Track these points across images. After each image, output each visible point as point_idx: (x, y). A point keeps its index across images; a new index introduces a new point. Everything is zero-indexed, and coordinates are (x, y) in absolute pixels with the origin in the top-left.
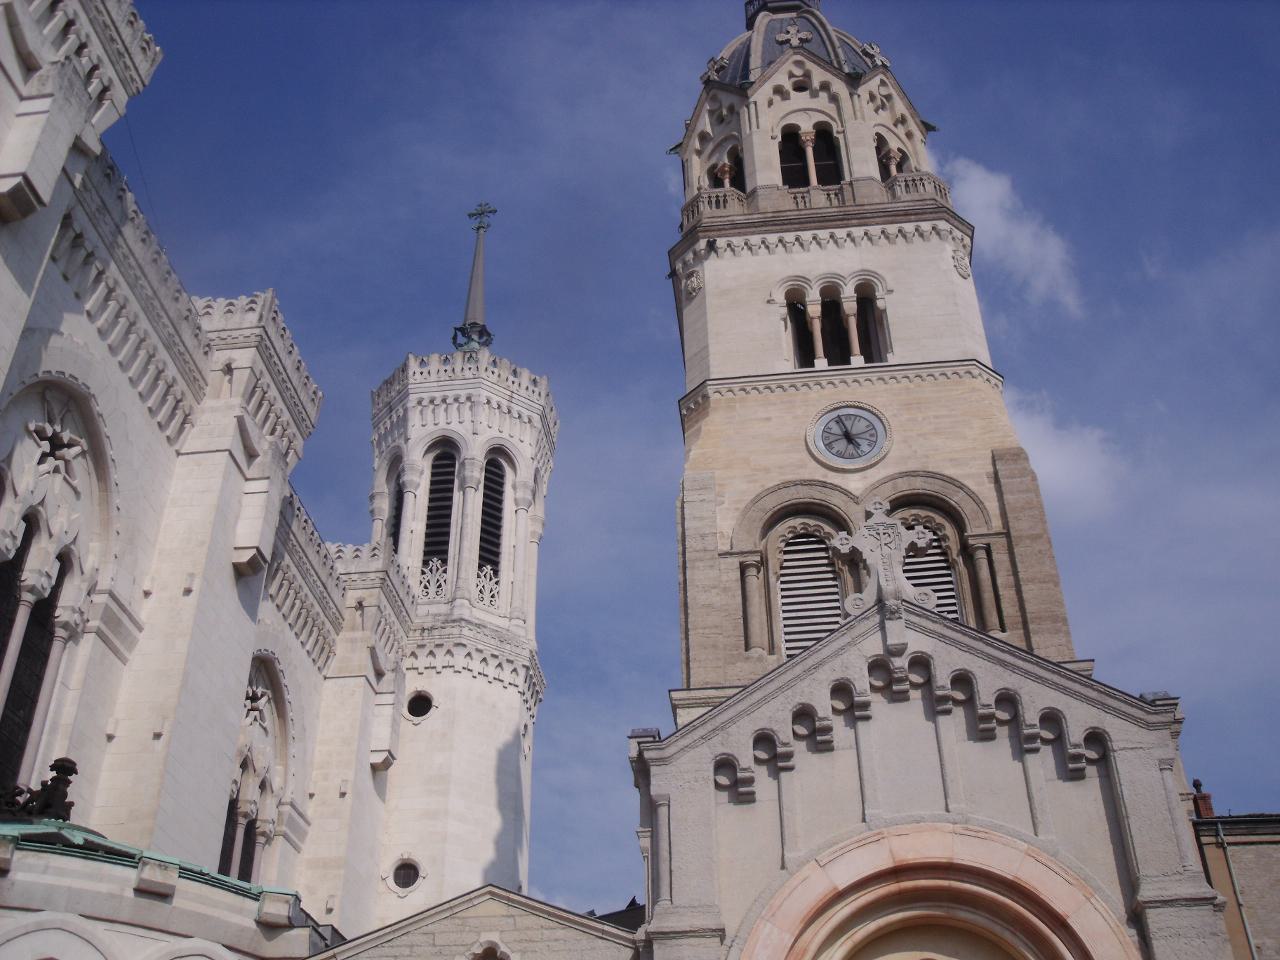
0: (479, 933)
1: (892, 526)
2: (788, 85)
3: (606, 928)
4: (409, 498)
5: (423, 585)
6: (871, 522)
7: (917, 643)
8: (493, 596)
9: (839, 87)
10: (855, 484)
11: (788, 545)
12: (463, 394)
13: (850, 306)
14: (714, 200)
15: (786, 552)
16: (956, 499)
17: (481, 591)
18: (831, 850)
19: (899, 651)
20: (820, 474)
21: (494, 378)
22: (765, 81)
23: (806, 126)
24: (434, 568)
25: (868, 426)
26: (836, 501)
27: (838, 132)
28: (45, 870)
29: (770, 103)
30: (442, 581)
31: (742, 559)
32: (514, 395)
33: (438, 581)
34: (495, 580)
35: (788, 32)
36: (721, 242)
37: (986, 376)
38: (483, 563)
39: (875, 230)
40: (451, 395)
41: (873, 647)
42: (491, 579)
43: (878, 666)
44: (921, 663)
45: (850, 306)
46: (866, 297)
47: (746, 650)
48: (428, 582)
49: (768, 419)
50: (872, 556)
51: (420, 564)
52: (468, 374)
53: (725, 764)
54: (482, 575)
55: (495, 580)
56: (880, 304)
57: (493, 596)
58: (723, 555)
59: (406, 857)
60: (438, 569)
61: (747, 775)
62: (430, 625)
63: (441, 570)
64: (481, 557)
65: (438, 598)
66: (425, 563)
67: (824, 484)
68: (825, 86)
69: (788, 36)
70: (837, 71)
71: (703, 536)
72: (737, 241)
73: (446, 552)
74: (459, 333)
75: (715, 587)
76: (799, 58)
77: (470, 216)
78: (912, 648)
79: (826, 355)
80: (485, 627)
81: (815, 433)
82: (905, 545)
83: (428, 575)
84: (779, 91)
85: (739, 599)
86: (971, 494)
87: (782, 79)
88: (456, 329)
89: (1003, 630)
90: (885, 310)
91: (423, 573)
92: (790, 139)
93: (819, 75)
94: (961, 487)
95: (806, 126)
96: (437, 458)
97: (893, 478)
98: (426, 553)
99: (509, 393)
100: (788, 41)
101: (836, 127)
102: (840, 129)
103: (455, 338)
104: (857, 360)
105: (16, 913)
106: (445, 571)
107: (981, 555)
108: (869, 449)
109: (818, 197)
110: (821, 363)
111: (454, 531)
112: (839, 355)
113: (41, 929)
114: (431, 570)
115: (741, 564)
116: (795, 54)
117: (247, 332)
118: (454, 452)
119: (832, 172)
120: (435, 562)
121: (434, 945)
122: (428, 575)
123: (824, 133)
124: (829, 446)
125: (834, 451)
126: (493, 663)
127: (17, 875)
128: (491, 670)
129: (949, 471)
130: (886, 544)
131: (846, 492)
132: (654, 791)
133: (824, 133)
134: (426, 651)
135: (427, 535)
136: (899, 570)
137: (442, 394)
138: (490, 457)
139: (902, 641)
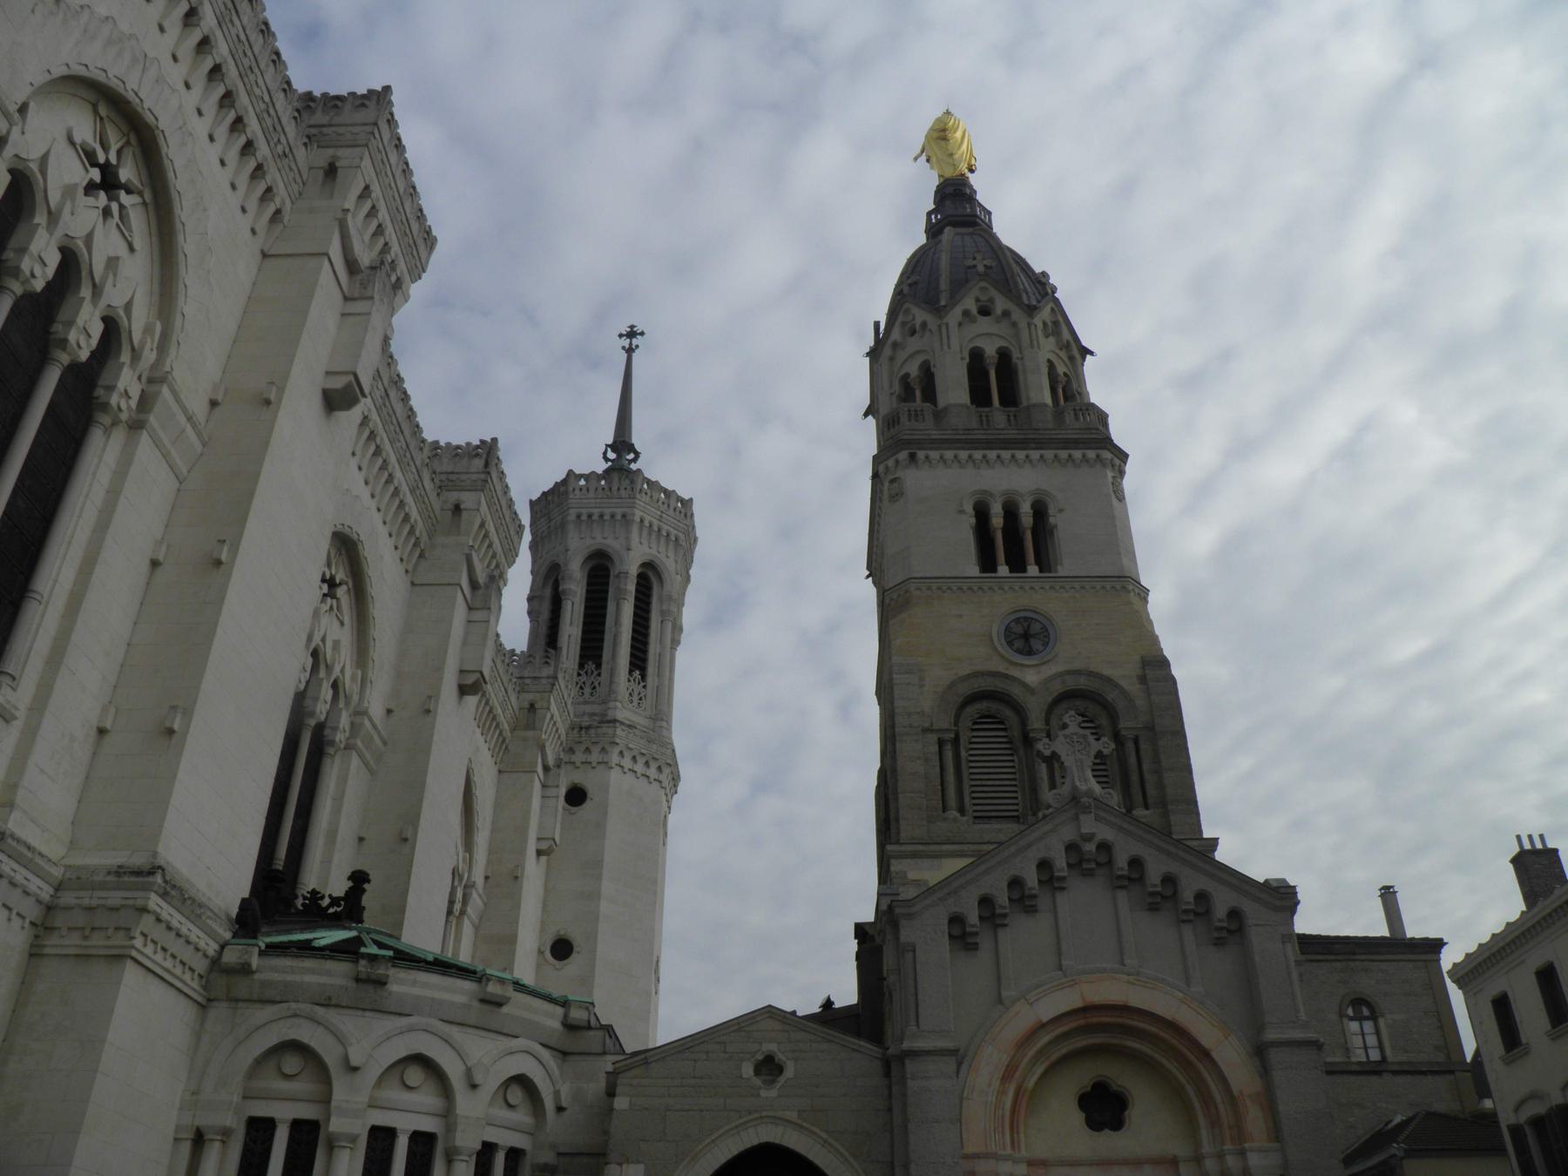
0: (761, 1043)
1: (1084, 737)
2: (974, 311)
3: (862, 1043)
5: (579, 686)
6: (1067, 732)
7: (1105, 833)
8: (640, 699)
9: (1017, 314)
10: (1032, 677)
11: (975, 723)
12: (619, 512)
13: (1027, 519)
14: (913, 413)
15: (973, 730)
16: (1111, 696)
17: (630, 694)
18: (1038, 991)
19: (1088, 838)
20: (1001, 668)
21: (647, 499)
22: (956, 304)
23: (990, 349)
24: (590, 671)
25: (1042, 629)
26: (1016, 691)
27: (1018, 359)
28: (414, 983)
29: (960, 324)
30: (596, 684)
31: (940, 736)
32: (664, 516)
33: (593, 683)
34: (642, 684)
35: (975, 259)
36: (921, 454)
37: (1137, 591)
38: (633, 669)
39: (1049, 454)
40: (607, 512)
41: (1068, 834)
42: (639, 683)
43: (1071, 848)
44: (1104, 847)
45: (1027, 519)
46: (1040, 511)
47: (944, 812)
48: (584, 683)
49: (961, 616)
50: (1068, 760)
51: (576, 667)
53: (956, 920)
54: (632, 679)
55: (642, 684)
56: (1052, 520)
57: (640, 699)
58: (926, 731)
59: (562, 933)
60: (592, 672)
61: (974, 929)
62: (587, 724)
63: (596, 673)
64: (631, 663)
65: (593, 699)
66: (581, 666)
67: (1006, 676)
68: (1006, 314)
69: (975, 262)
70: (1017, 300)
71: (909, 714)
72: (934, 455)
73: (600, 657)
74: (609, 449)
75: (919, 758)
76: (983, 284)
77: (621, 336)
78: (1099, 837)
79: (1007, 563)
80: (636, 728)
81: (996, 629)
82: (1093, 753)
83: (584, 678)
84: (966, 313)
85: (938, 769)
86: (1123, 692)
87: (969, 303)
88: (607, 446)
89: (1147, 807)
90: (1056, 526)
91: (579, 675)
92: (976, 357)
93: (1001, 304)
94: (1116, 686)
95: (990, 349)
97: (1061, 674)
98: (582, 657)
99: (659, 513)
100: (975, 266)
101: (1015, 355)
102: (1020, 356)
103: (605, 453)
104: (1033, 570)
105: (392, 1017)
106: (599, 675)
107: (1130, 746)
108: (1042, 648)
109: (998, 414)
110: (1003, 570)
111: (608, 638)
112: (1017, 565)
113: (411, 1029)
114: (586, 673)
115: (939, 739)
116: (981, 280)
117: (474, 477)
118: (609, 565)
119: (1010, 397)
120: (591, 666)
121: (725, 1052)
122: (584, 678)
123: (1004, 356)
124: (1010, 644)
125: (1014, 648)
126: (641, 761)
127: (394, 988)
128: (639, 768)
129: (1107, 672)
130: (1079, 751)
131: (1025, 685)
132: (903, 939)
133: (1004, 356)
134: (583, 747)
135: (583, 640)
136: (1089, 774)
137: (599, 510)
138: (640, 571)
139: (1092, 831)
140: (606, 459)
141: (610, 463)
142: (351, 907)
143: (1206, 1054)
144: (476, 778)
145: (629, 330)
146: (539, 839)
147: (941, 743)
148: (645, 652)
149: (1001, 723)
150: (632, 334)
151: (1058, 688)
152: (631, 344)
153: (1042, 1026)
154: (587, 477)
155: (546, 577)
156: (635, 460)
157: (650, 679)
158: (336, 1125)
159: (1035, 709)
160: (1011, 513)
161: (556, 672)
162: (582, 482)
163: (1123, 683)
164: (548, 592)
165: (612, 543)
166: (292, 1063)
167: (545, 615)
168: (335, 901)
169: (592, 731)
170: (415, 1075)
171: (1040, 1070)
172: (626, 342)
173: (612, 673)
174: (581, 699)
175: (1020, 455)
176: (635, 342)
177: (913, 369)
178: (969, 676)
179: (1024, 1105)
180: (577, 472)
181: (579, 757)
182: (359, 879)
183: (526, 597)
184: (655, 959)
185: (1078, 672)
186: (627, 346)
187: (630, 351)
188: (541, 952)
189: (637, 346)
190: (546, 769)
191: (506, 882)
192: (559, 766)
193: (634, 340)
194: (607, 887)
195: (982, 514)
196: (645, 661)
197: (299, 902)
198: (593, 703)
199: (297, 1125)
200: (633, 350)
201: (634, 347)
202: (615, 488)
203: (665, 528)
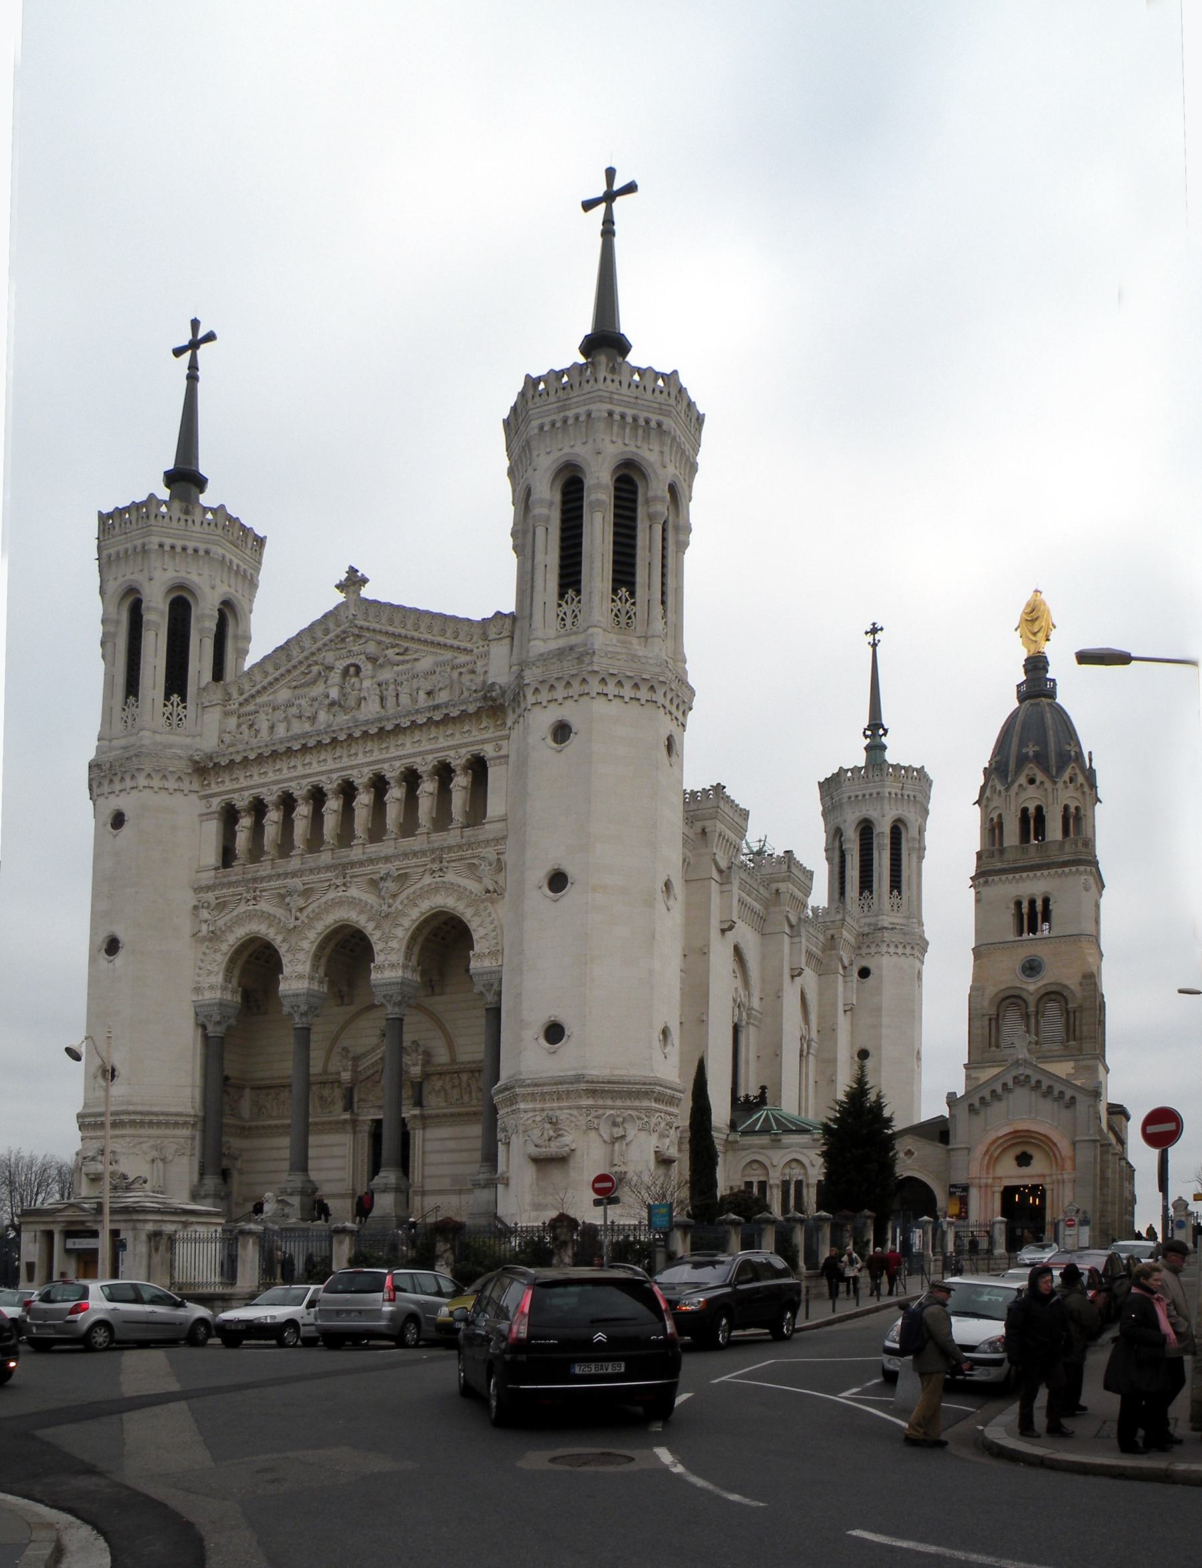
4: (848, 858)
10: (1032, 988)
26: (1024, 995)
43: (1015, 1078)
44: (1028, 1076)
46: (1046, 901)
52: (877, 779)
66: (861, 894)
77: (867, 633)
78: (1026, 1073)
81: (1018, 966)
83: (863, 902)
88: (865, 729)
91: (860, 900)
96: (862, 829)
97: (1045, 985)
98: (860, 888)
103: (864, 733)
106: (872, 898)
111: (875, 874)
122: (863, 902)
124: (1024, 972)
131: (1028, 991)
134: (865, 946)
135: (860, 877)
140: (866, 737)
141: (868, 739)
142: (762, 1100)
143: (1055, 1144)
144: (807, 991)
145: (872, 627)
146: (844, 1005)
147: (990, 1020)
148: (900, 876)
149: (1019, 1006)
150: (874, 630)
151: (1043, 991)
152: (874, 640)
153: (1000, 1138)
154: (852, 770)
155: (835, 836)
156: (885, 734)
157: (903, 893)
158: (771, 1182)
159: (1032, 1001)
160: (1032, 903)
161: (844, 916)
162: (849, 774)
163: (1072, 987)
164: (837, 844)
165: (873, 814)
166: (755, 1166)
167: (837, 860)
168: (755, 1098)
169: (870, 936)
170: (794, 1165)
171: (999, 1151)
172: (870, 638)
173: (879, 896)
174: (862, 915)
175: (1038, 873)
176: (877, 637)
177: (995, 815)
178: (1006, 989)
179: (993, 1161)
180: (845, 768)
181: (864, 951)
182: (763, 1088)
183: (823, 849)
184: (916, 1051)
185: (1052, 984)
186: (872, 642)
187: (874, 645)
188: (852, 1058)
189: (879, 641)
190: (844, 968)
191: (828, 1032)
192: (851, 965)
193: (876, 635)
194: (885, 1020)
195: (1018, 904)
196: (899, 882)
197: (742, 1099)
198: (870, 916)
199: (760, 1182)
200: (876, 645)
201: (876, 642)
202: (870, 776)
203: (906, 793)
